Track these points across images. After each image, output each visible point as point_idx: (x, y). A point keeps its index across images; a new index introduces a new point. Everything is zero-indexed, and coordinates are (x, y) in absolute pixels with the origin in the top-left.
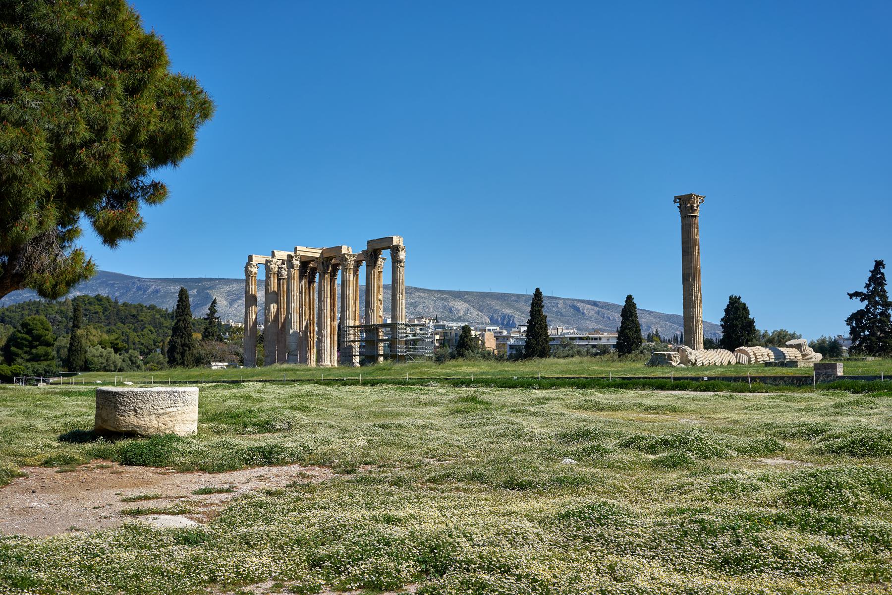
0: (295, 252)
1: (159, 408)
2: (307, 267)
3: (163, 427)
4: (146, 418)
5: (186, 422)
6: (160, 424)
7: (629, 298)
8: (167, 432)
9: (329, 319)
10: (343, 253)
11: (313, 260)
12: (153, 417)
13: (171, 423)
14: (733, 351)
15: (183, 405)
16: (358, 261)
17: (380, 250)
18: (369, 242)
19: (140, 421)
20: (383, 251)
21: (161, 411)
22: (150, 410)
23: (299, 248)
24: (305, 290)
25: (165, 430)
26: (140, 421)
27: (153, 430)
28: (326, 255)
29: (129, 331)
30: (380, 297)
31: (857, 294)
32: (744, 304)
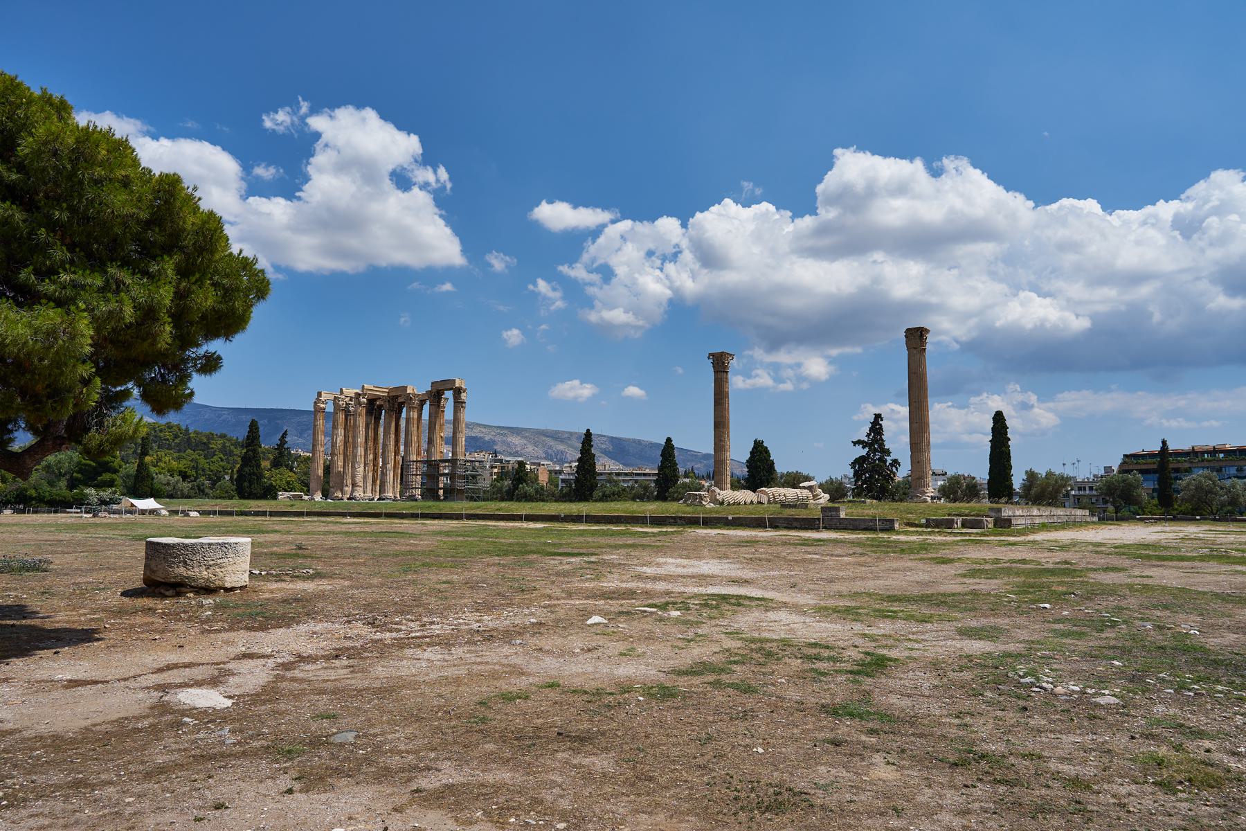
2: (374, 405)
4: (197, 570)
7: (669, 440)
8: (217, 582)
11: (379, 398)
14: (754, 491)
16: (421, 401)
18: (432, 383)
19: (190, 573)
21: (212, 563)
24: (372, 426)
26: (190, 573)
28: (391, 394)
30: (442, 434)
31: (859, 442)
32: (766, 448)
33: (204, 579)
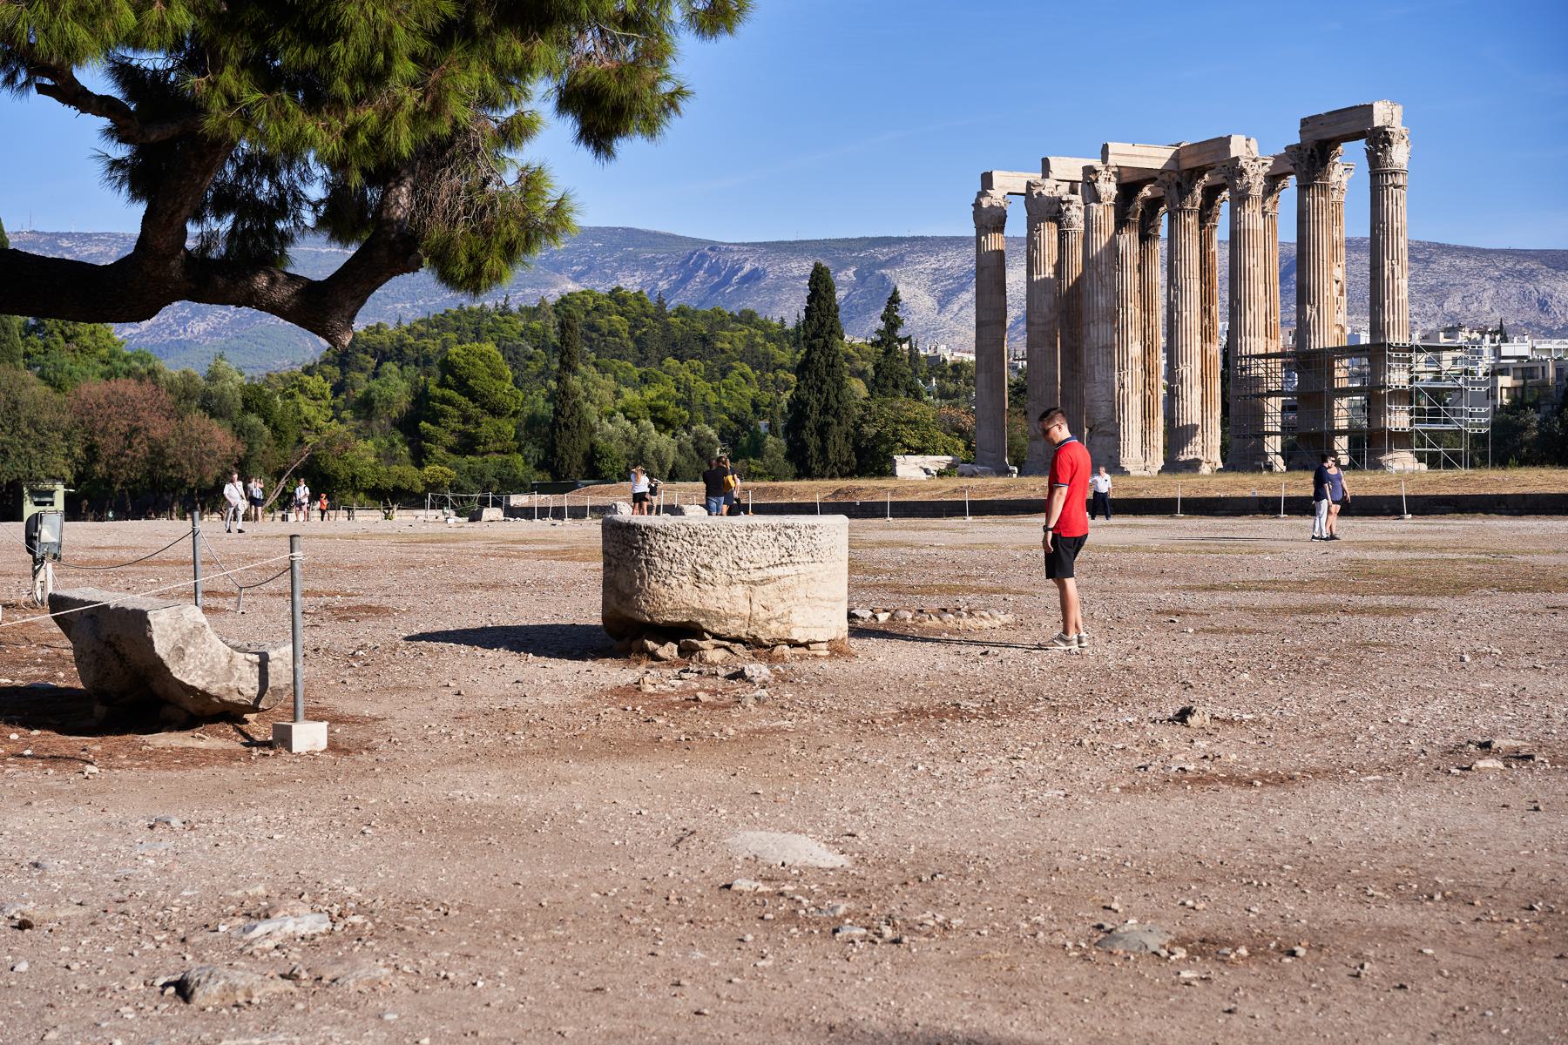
0: (1105, 159)
1: (753, 565)
3: (763, 615)
5: (819, 603)
6: (755, 607)
8: (774, 625)
9: (1198, 337)
11: (1148, 177)
12: (739, 590)
13: (782, 605)
15: (811, 559)
17: (1336, 142)
18: (1304, 122)
21: (757, 575)
22: (730, 571)
23: (1113, 147)
25: (768, 621)
27: (739, 622)
29: (692, 377)
33: (739, 616)
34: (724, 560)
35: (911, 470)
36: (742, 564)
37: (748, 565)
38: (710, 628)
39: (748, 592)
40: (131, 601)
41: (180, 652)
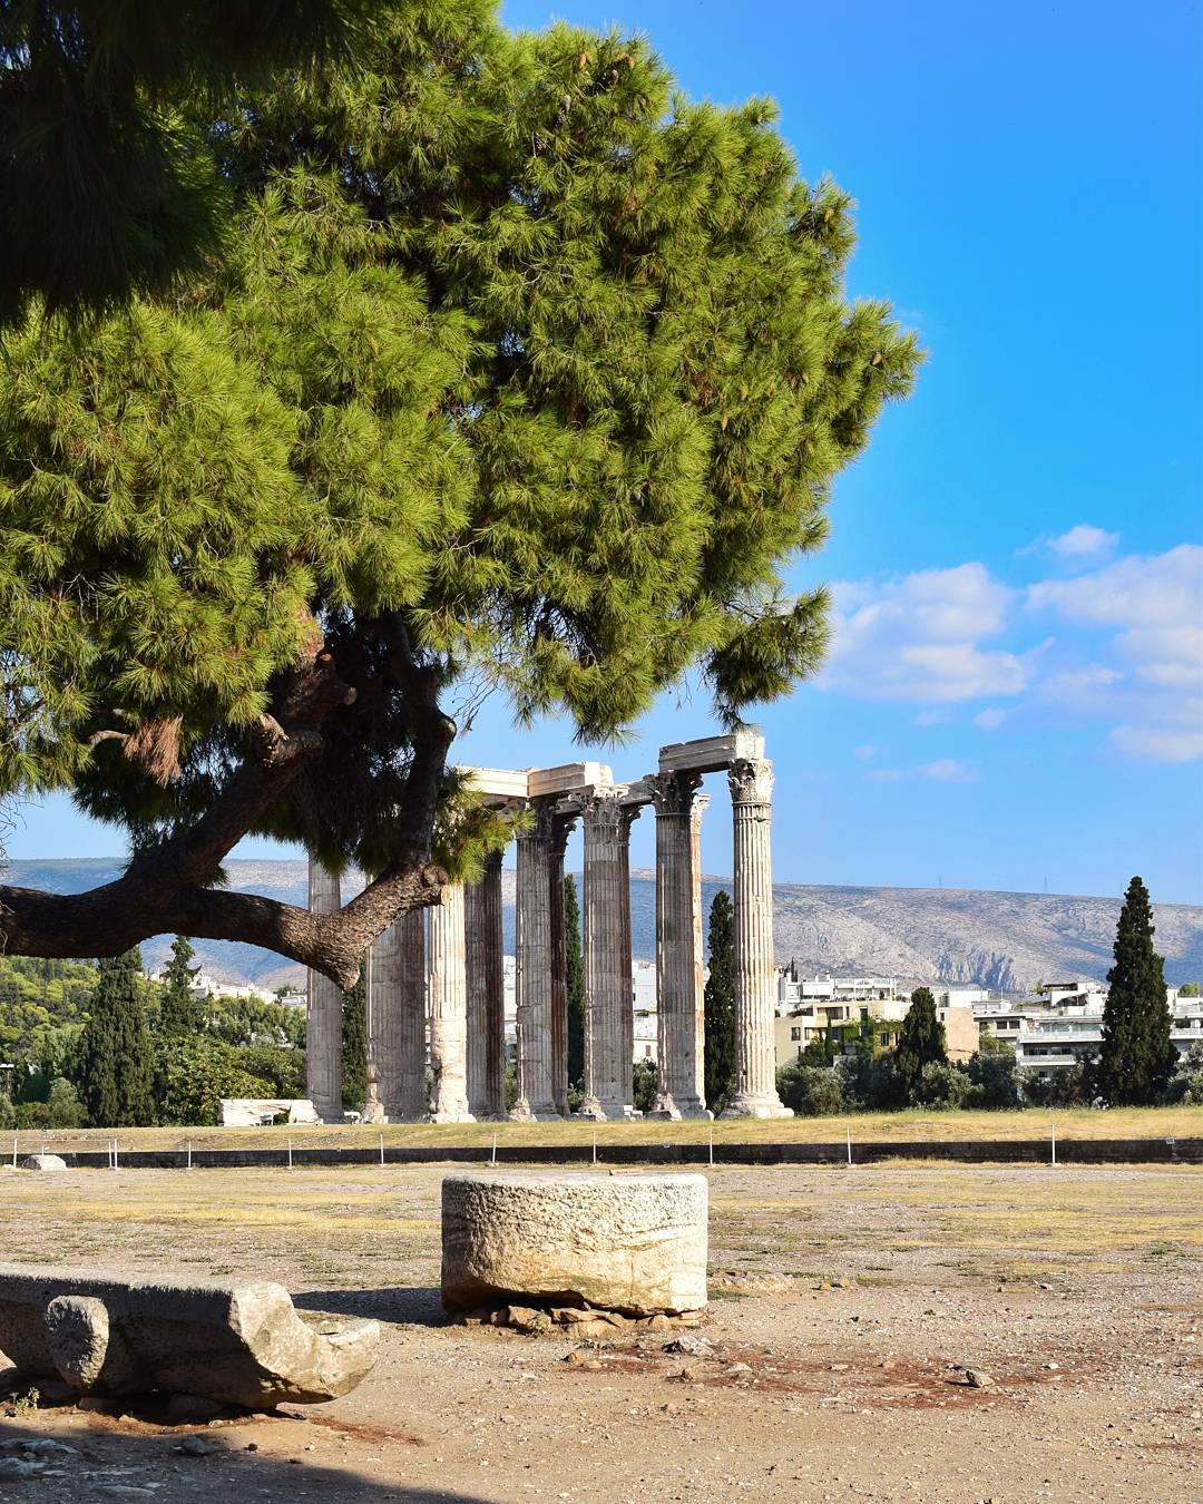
6: (637, 1274)
8: (656, 1294)
10: (587, 784)
13: (662, 1272)
18: (664, 751)
20: (704, 777)
21: (639, 1240)
22: (612, 1236)
25: (649, 1289)
27: (622, 1291)
34: (606, 1224)
35: (242, 1116)
36: (624, 1227)
37: (631, 1229)
38: (591, 1298)
39: (630, 1258)
40: (206, 1282)
41: (265, 1335)
